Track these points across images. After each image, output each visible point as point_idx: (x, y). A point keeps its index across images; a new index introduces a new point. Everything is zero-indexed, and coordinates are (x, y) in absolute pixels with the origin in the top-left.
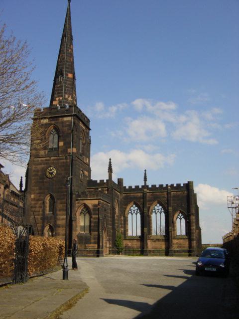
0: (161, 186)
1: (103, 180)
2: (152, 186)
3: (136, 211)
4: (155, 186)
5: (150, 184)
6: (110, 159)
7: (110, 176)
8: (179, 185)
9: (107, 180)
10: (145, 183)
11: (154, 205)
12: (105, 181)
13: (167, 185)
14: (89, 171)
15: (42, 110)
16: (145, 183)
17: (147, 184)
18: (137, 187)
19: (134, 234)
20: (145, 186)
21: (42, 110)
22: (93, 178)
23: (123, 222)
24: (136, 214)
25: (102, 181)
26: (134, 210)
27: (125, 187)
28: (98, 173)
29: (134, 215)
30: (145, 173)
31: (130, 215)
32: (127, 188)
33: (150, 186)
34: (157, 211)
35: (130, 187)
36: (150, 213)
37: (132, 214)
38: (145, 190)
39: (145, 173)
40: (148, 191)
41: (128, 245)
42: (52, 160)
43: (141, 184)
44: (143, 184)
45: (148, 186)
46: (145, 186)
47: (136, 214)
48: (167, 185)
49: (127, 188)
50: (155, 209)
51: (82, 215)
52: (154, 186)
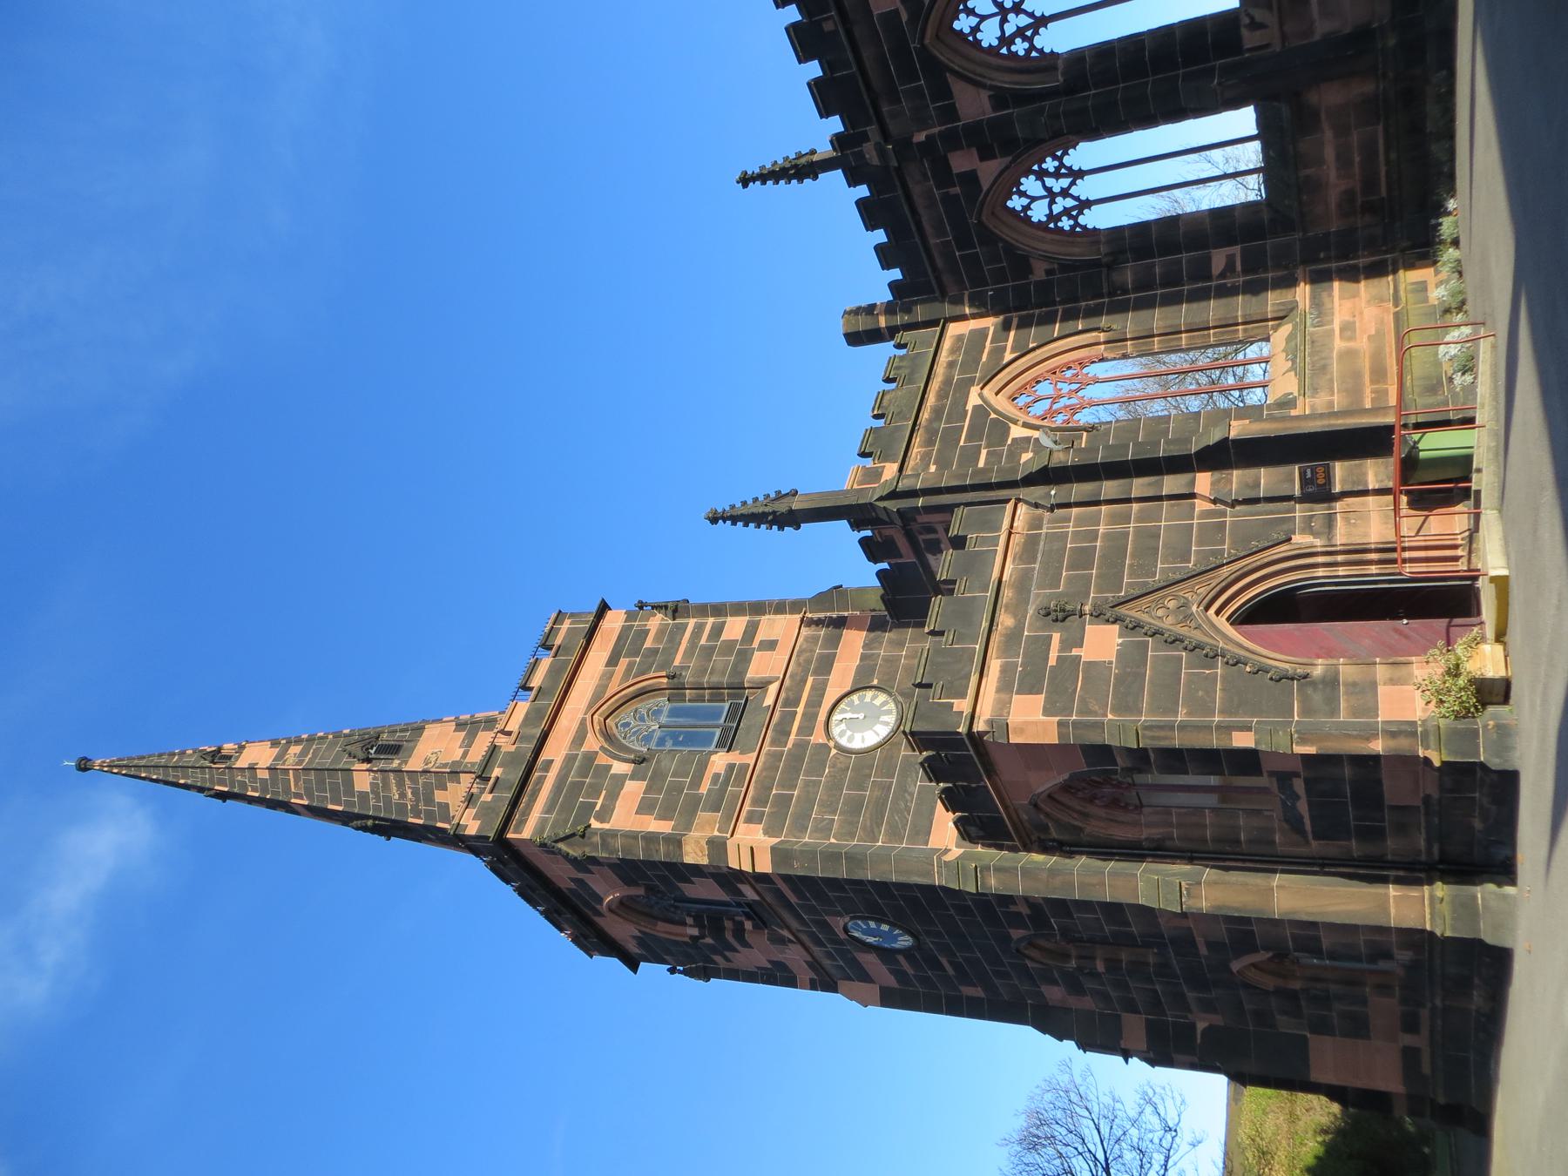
0: (804, 41)
2: (825, 112)
3: (1057, 185)
4: (816, 87)
5: (821, 133)
11: (969, 42)
16: (827, 165)
17: (825, 149)
18: (870, 213)
19: (1251, 155)
23: (1158, 265)
24: (1078, 174)
26: (1051, 195)
27: (893, 286)
29: (1084, 189)
30: (763, 177)
31: (1096, 219)
33: (835, 124)
34: (1016, 22)
35: (886, 256)
36: (1038, 84)
37: (1085, 204)
38: (870, 152)
39: (763, 177)
40: (872, 130)
41: (1349, 195)
43: (837, 195)
44: (837, 177)
45: (838, 141)
46: (847, 157)
47: (1078, 174)
50: (1006, 40)
52: (826, 96)
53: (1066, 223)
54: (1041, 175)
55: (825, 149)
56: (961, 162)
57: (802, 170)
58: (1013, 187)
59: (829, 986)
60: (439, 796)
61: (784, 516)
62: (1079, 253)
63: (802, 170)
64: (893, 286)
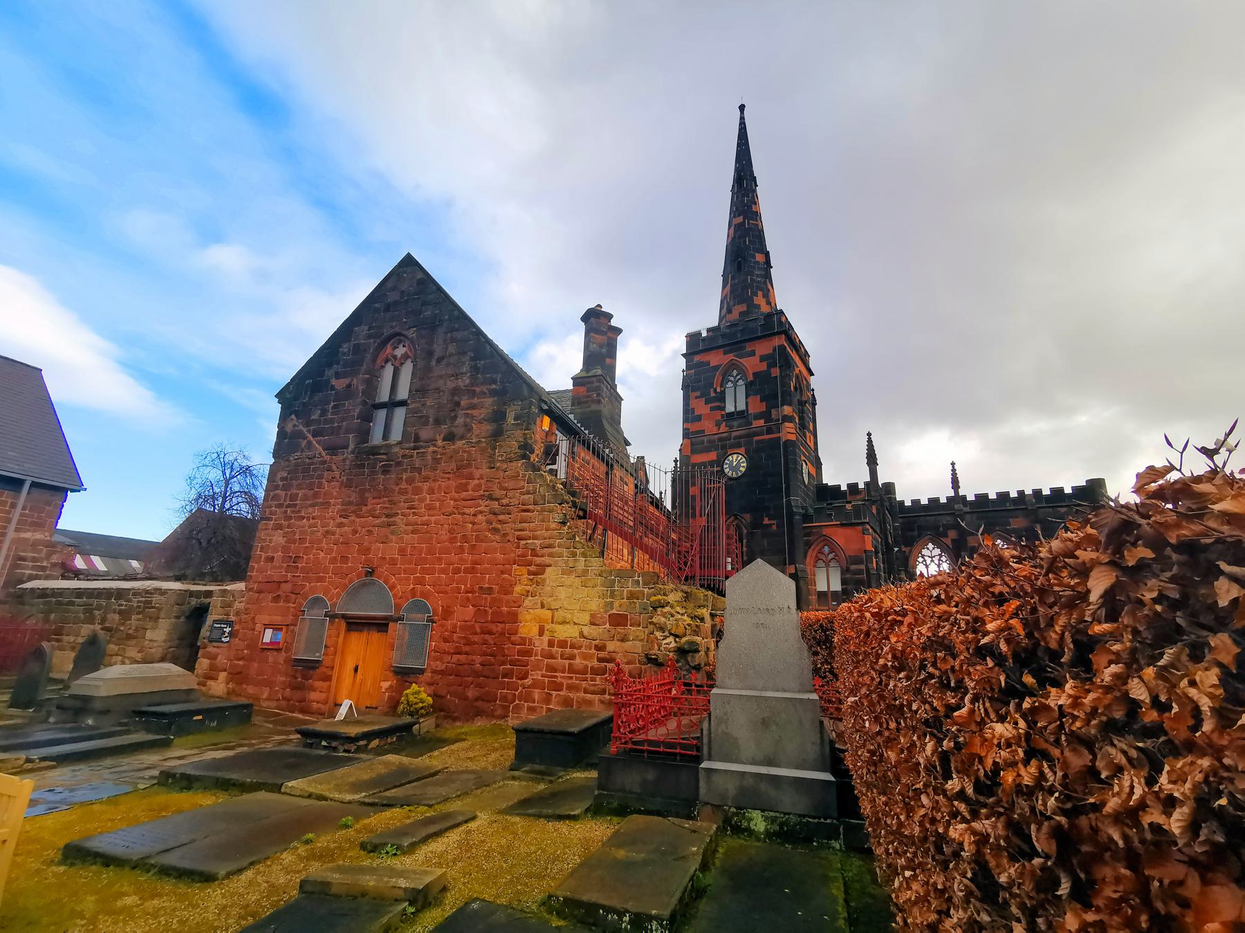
0: (1003, 496)
1: (857, 484)
5: (969, 491)
6: (869, 434)
7: (873, 473)
8: (1057, 493)
9: (867, 484)
10: (956, 491)
12: (861, 486)
13: (1021, 493)
14: (818, 464)
15: (704, 334)
16: (956, 491)
17: (961, 493)
18: (934, 502)
20: (957, 499)
21: (704, 334)
22: (829, 478)
25: (853, 487)
27: (903, 502)
28: (840, 468)
32: (908, 503)
33: (971, 498)
40: (967, 509)
42: (735, 438)
43: (944, 493)
44: (952, 494)
45: (964, 497)
46: (957, 499)
48: (1021, 493)
49: (908, 503)
51: (820, 563)
52: (982, 499)
53: (920, 559)
54: (940, 556)
55: (961, 493)
56: (953, 534)
57: (955, 483)
58: (937, 544)
59: (686, 434)
60: (760, 293)
61: (872, 459)
62: (911, 562)
63: (955, 483)
64: (903, 502)
